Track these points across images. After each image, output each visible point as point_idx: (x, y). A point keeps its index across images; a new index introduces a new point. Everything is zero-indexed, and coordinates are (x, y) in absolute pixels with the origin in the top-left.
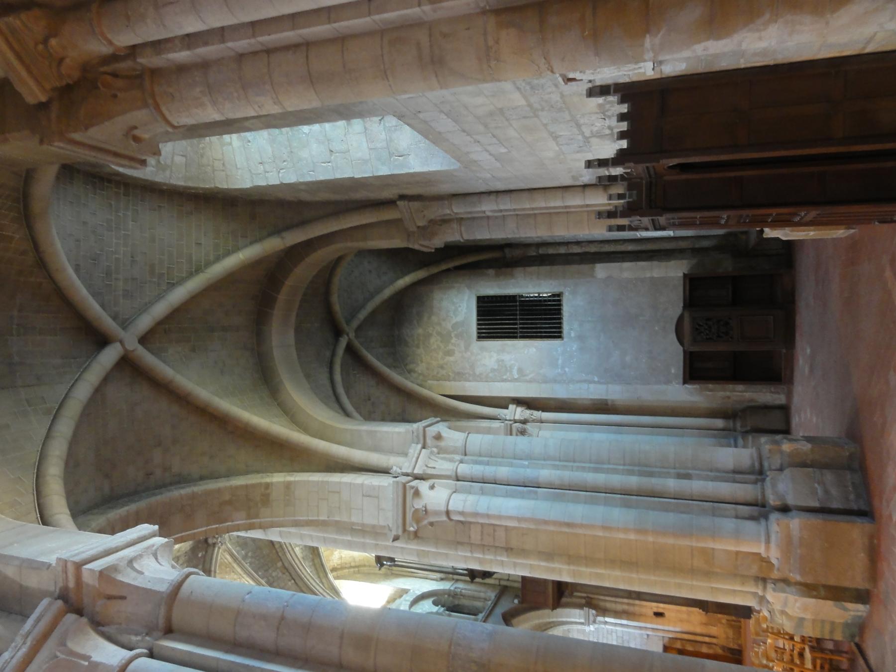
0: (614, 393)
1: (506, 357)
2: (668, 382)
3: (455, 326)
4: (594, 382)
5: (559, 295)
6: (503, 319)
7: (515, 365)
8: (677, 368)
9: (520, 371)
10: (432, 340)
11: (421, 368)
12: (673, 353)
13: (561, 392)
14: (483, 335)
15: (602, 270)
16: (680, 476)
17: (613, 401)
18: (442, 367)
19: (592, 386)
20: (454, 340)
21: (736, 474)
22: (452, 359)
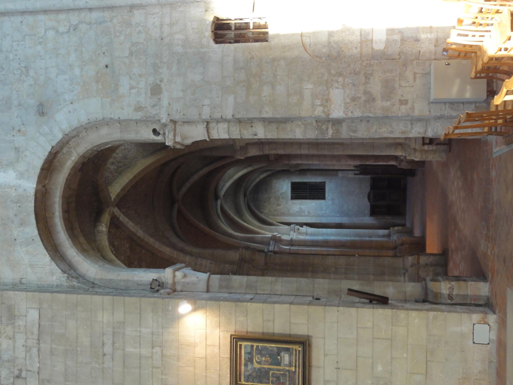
0: (344, 220)
1: (303, 207)
2: (364, 216)
3: (282, 194)
4: (337, 216)
5: (324, 183)
6: (300, 192)
7: (308, 209)
8: (368, 211)
9: (308, 212)
10: (272, 200)
11: (266, 211)
12: (366, 204)
13: (324, 220)
14: (293, 198)
15: (340, 174)
16: (369, 237)
17: (344, 224)
18: (276, 211)
19: (337, 218)
20: (281, 200)
21: (384, 236)
22: (280, 207)
